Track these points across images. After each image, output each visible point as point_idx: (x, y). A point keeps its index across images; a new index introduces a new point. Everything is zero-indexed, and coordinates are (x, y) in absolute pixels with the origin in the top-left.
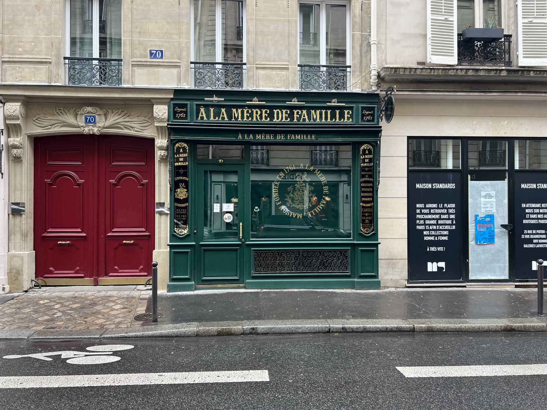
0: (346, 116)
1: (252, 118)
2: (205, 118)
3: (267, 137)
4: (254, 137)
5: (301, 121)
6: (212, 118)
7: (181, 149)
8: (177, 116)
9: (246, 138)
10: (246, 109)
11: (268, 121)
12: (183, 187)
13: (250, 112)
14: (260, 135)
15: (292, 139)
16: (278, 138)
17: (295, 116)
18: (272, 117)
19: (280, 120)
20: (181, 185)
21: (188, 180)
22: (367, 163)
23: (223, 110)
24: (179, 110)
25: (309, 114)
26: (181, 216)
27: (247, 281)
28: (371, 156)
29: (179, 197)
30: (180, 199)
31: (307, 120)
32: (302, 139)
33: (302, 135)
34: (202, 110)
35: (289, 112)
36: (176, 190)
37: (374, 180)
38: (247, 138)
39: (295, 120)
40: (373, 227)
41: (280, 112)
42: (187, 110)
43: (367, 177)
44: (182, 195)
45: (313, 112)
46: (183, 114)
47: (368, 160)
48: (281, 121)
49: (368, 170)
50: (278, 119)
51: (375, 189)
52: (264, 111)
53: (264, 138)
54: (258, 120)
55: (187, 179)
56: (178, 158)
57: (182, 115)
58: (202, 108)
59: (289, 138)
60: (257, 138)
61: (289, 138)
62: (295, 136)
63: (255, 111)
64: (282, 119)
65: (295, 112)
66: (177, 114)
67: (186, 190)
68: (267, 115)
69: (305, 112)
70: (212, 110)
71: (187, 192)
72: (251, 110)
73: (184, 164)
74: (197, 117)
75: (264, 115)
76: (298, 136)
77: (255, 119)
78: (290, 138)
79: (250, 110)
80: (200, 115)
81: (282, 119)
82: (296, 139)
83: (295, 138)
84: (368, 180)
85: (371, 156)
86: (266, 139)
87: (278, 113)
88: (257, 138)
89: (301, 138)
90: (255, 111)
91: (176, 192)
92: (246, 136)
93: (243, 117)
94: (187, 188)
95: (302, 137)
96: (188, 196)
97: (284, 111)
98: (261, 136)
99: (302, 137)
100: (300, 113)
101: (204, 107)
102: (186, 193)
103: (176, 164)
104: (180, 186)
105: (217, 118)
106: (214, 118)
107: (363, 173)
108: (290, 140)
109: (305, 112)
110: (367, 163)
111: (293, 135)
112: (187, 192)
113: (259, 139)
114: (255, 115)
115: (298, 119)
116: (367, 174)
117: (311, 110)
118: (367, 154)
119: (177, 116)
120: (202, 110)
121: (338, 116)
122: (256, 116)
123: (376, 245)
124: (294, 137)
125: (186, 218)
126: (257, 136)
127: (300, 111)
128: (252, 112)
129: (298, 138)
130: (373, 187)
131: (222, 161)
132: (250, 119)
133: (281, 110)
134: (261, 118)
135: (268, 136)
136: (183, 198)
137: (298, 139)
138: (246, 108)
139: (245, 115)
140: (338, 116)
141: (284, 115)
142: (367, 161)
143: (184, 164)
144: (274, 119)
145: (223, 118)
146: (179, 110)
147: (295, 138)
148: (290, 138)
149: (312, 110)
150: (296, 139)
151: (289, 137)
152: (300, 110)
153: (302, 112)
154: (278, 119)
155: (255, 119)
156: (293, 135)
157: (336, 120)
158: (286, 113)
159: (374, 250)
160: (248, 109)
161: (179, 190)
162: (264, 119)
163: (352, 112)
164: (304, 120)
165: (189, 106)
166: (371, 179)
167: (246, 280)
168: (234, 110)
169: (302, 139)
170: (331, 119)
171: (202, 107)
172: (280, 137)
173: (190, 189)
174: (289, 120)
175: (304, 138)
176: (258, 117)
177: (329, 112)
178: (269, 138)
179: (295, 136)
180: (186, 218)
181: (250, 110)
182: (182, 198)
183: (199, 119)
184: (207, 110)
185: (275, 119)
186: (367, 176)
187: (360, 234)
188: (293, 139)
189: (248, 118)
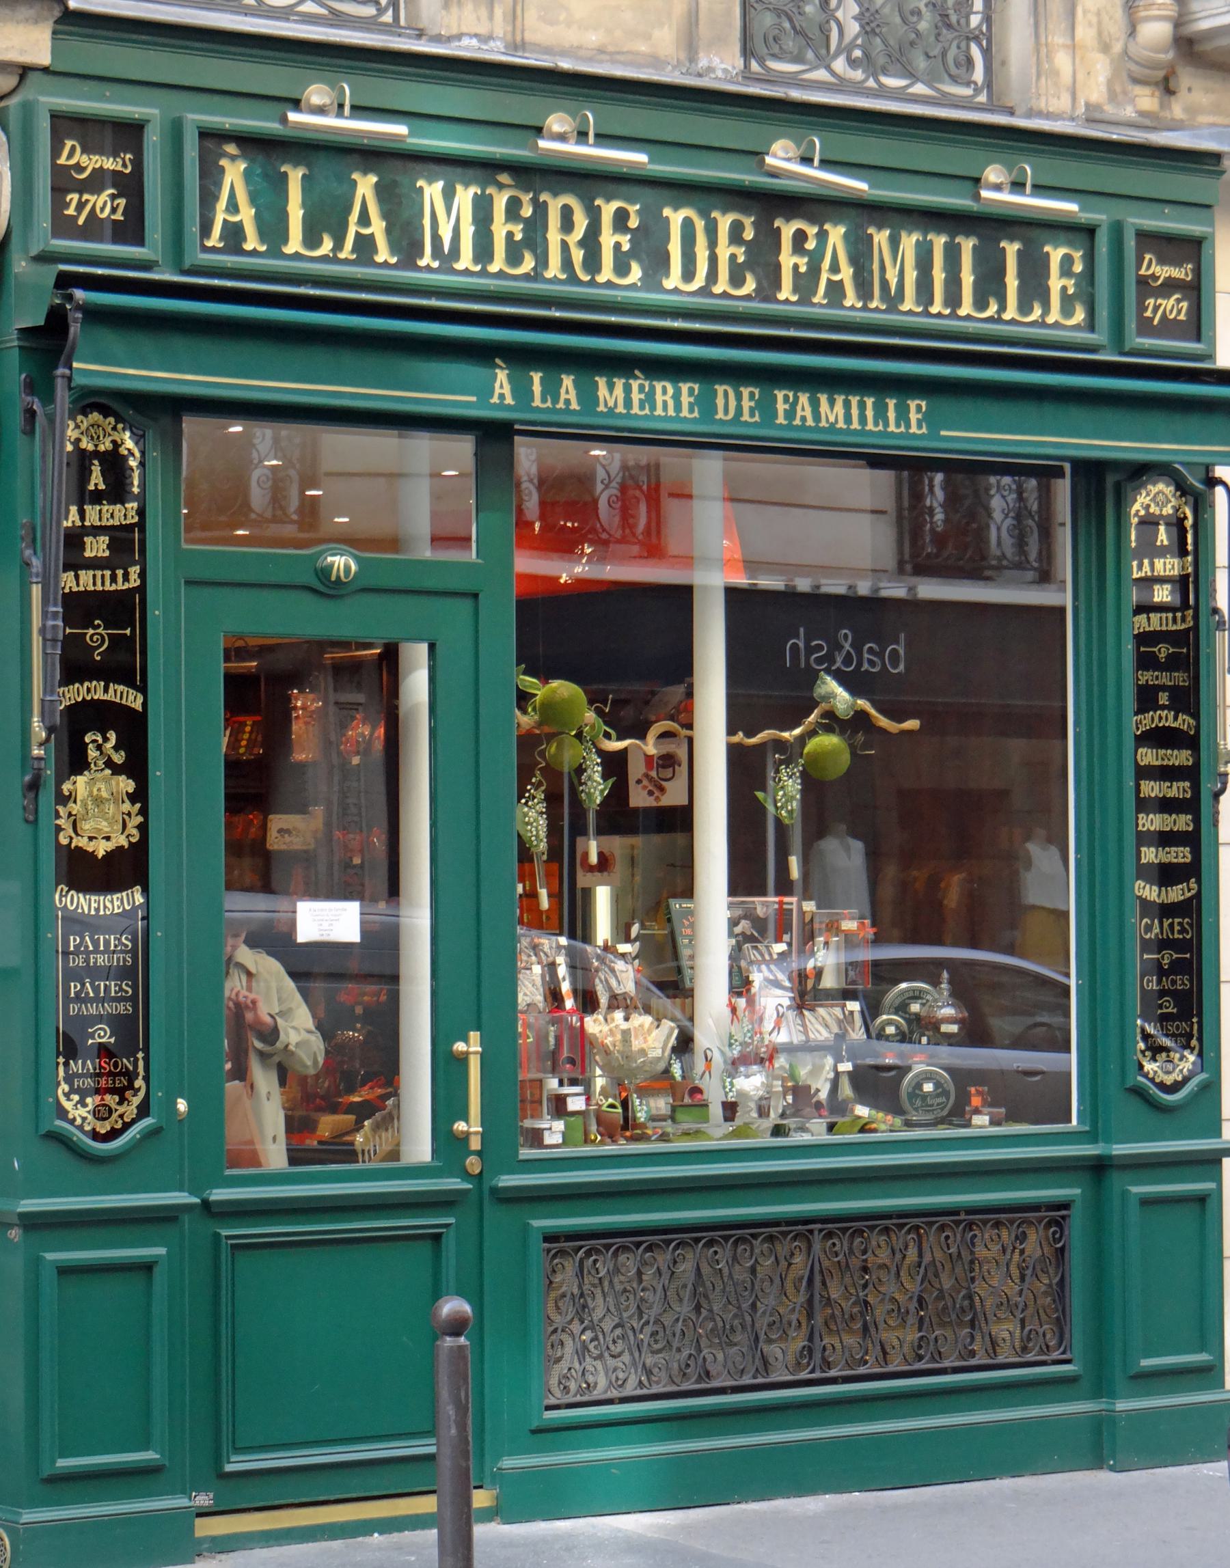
0: (1056, 283)
1: (542, 261)
2: (383, 254)
3: (659, 398)
4: (588, 396)
5: (819, 298)
6: (295, 245)
7: (96, 470)
8: (71, 211)
9: (537, 402)
10: (501, 187)
11: (632, 287)
12: (109, 764)
13: (527, 211)
14: (840, 399)
15: (797, 422)
16: (720, 415)
17: (788, 260)
18: (658, 263)
19: (699, 281)
20: (99, 747)
21: (138, 706)
22: (95, 564)
23: (365, 185)
24: (84, 160)
25: (860, 254)
26: (96, 989)
27: (508, 1463)
28: (122, 514)
29: (82, 842)
30: (93, 855)
31: (851, 299)
32: (855, 425)
33: (891, 403)
34: (234, 173)
35: (749, 234)
36: (66, 787)
37: (1198, 728)
38: (544, 400)
39: (786, 293)
40: (1200, 1040)
41: (700, 224)
42: (138, 164)
43: (1163, 707)
44: (104, 826)
45: (881, 238)
46: (113, 197)
47: (104, 540)
48: (705, 291)
49: (1169, 656)
50: (689, 275)
51: (1206, 787)
52: (609, 210)
53: (642, 408)
54: (573, 279)
55: (134, 700)
56: (74, 540)
57: (104, 203)
58: (233, 158)
59: (781, 420)
60: (601, 408)
61: (781, 420)
62: (815, 404)
63: (555, 206)
64: (712, 276)
65: (788, 230)
66: (75, 196)
67: (126, 785)
68: (625, 241)
69: (836, 234)
70: (295, 176)
71: (133, 797)
72: (535, 201)
73: (114, 579)
74: (206, 230)
75: (608, 239)
76: (832, 403)
77: (554, 269)
78: (790, 414)
79: (526, 198)
80: (220, 217)
81: (712, 276)
82: (823, 424)
83: (817, 416)
84: (1170, 723)
85: (122, 514)
86: (554, 411)
87: (688, 225)
88: (601, 408)
89: (848, 418)
90: (555, 206)
91: (63, 799)
92: (537, 388)
93: (483, 251)
94: (136, 767)
95: (855, 412)
96: (143, 828)
97: (725, 222)
98: (628, 390)
99: (855, 412)
100: (811, 245)
101: (244, 156)
102: (127, 806)
103: (68, 581)
104: (92, 753)
105: (327, 246)
106: (311, 240)
107: (1147, 677)
108: (790, 427)
109: (836, 234)
110: (95, 564)
111: (804, 399)
112: (133, 797)
113: (611, 410)
114: (554, 236)
115: (805, 283)
116: (1163, 688)
117: (871, 230)
118: (97, 497)
119: (71, 211)
120: (234, 173)
121: (1012, 283)
122: (565, 246)
123: (1210, 1162)
124: (808, 413)
125: (133, 999)
126: (603, 391)
127: (812, 230)
128: (541, 209)
129: (832, 419)
130: (1191, 774)
131: (347, 569)
132: (528, 264)
133: (705, 214)
134: (592, 262)
135: (665, 392)
136: (110, 846)
137: (832, 428)
138: (504, 178)
139: (500, 229)
140: (1012, 283)
141: (724, 251)
142: (97, 547)
143: (114, 579)
144: (667, 275)
145: (365, 245)
146: (84, 160)
147: (817, 416)
148: (790, 414)
149: (880, 228)
150: (823, 424)
151: (781, 407)
152: (812, 220)
153: (822, 236)
154: (689, 275)
155: (554, 269)
156: (804, 399)
157: (1003, 308)
158: (736, 235)
159: (1201, 1200)
160: (515, 187)
161: (81, 780)
162: (607, 273)
163: (1090, 259)
164: (835, 289)
165: (153, 139)
166: (1183, 722)
167: (499, 1457)
168: (432, 191)
169: (855, 425)
170: (981, 304)
171: (231, 149)
172: (733, 403)
173: (157, 773)
174: (750, 286)
175: (863, 419)
176: (578, 255)
177: (968, 245)
178: (671, 412)
179: (815, 404)
180: (133, 999)
181: (526, 198)
182: (101, 849)
183: (214, 241)
184: (266, 176)
185: (673, 280)
186: (1163, 698)
187: (1139, 1092)
188: (802, 427)
189: (514, 255)
